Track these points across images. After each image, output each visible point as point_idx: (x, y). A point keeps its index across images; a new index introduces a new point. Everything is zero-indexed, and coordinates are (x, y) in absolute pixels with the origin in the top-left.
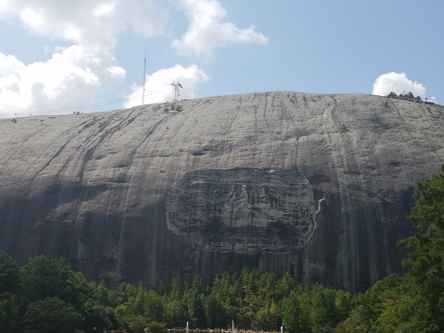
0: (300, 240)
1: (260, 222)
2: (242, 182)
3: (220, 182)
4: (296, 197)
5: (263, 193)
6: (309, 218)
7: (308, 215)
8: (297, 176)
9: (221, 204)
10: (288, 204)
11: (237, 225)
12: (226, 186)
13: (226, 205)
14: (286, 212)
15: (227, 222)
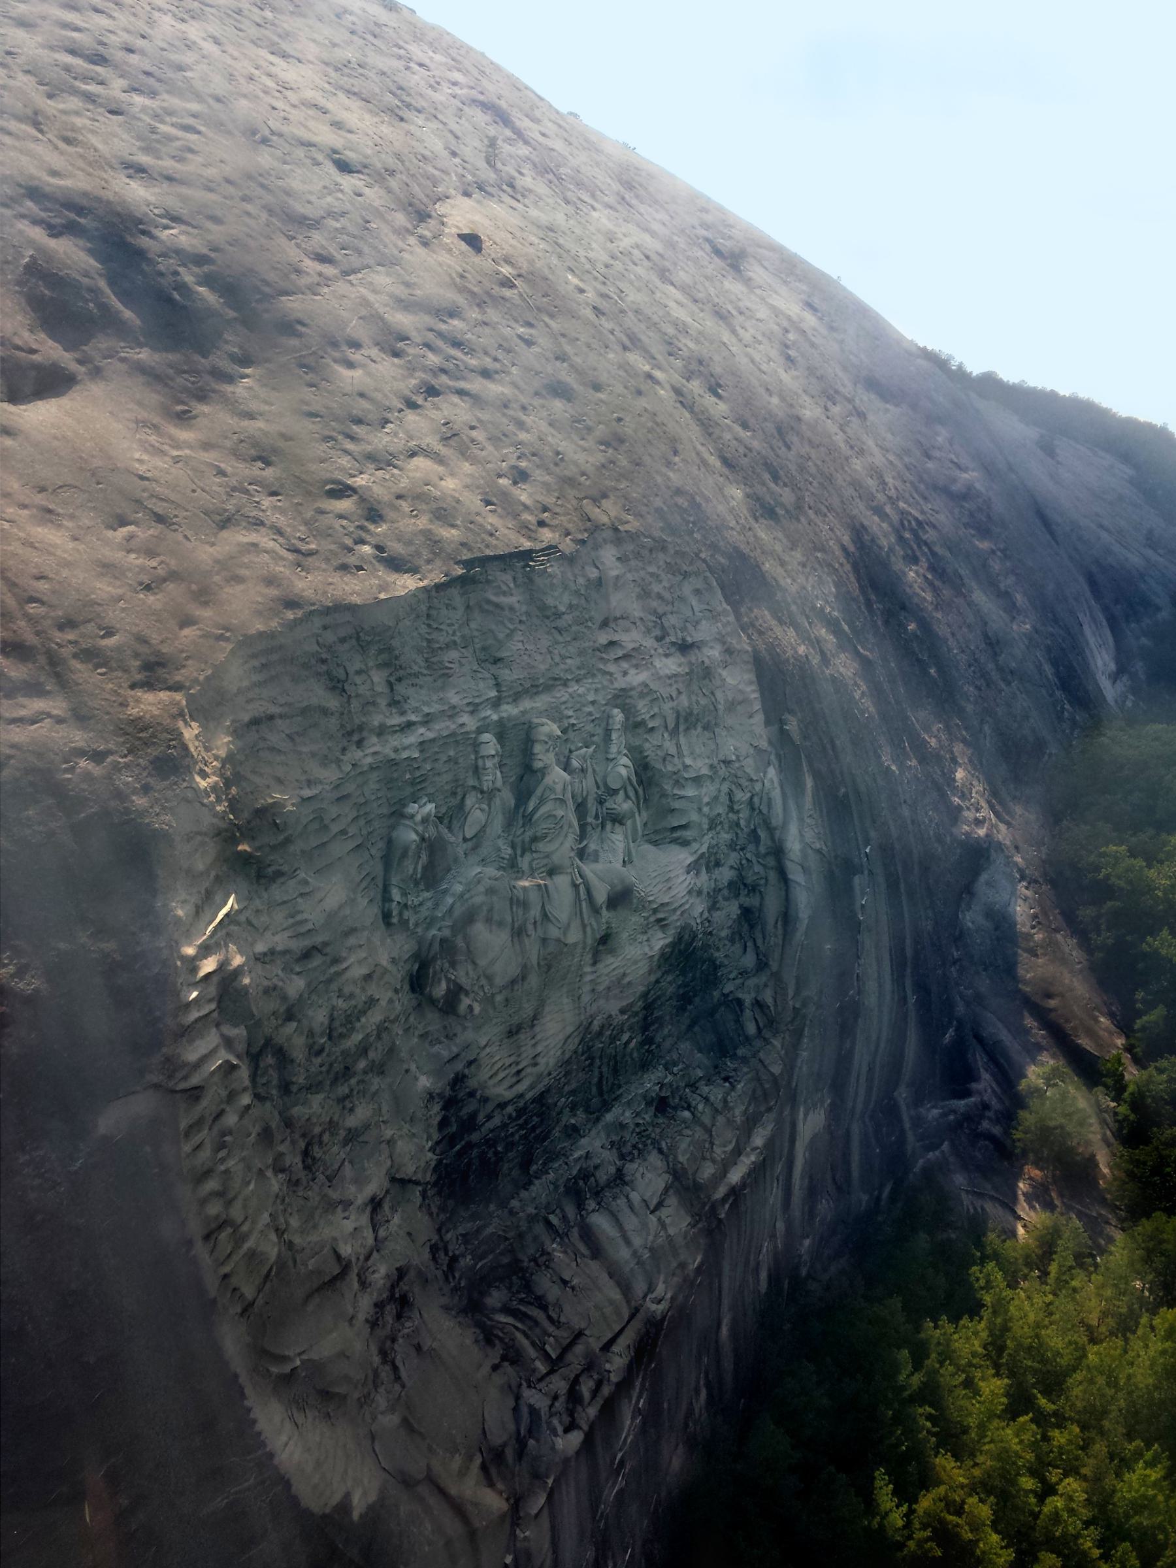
0: (748, 999)
1: (624, 975)
2: (526, 691)
3: (410, 724)
4: (706, 728)
5: (614, 749)
6: (762, 850)
7: (754, 831)
8: (686, 575)
9: (460, 943)
10: (690, 792)
11: (542, 1061)
12: (452, 753)
13: (479, 929)
14: (685, 843)
15: (501, 1075)
